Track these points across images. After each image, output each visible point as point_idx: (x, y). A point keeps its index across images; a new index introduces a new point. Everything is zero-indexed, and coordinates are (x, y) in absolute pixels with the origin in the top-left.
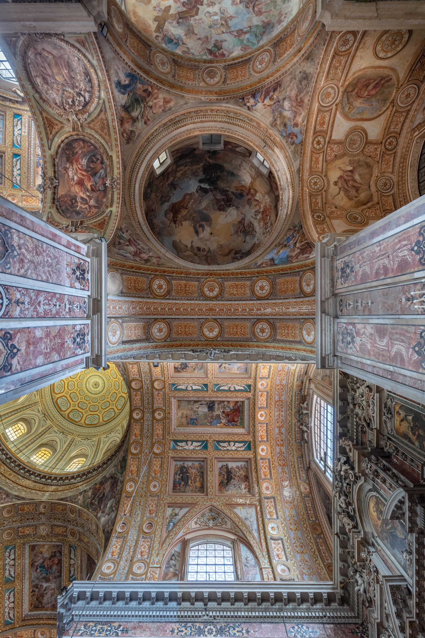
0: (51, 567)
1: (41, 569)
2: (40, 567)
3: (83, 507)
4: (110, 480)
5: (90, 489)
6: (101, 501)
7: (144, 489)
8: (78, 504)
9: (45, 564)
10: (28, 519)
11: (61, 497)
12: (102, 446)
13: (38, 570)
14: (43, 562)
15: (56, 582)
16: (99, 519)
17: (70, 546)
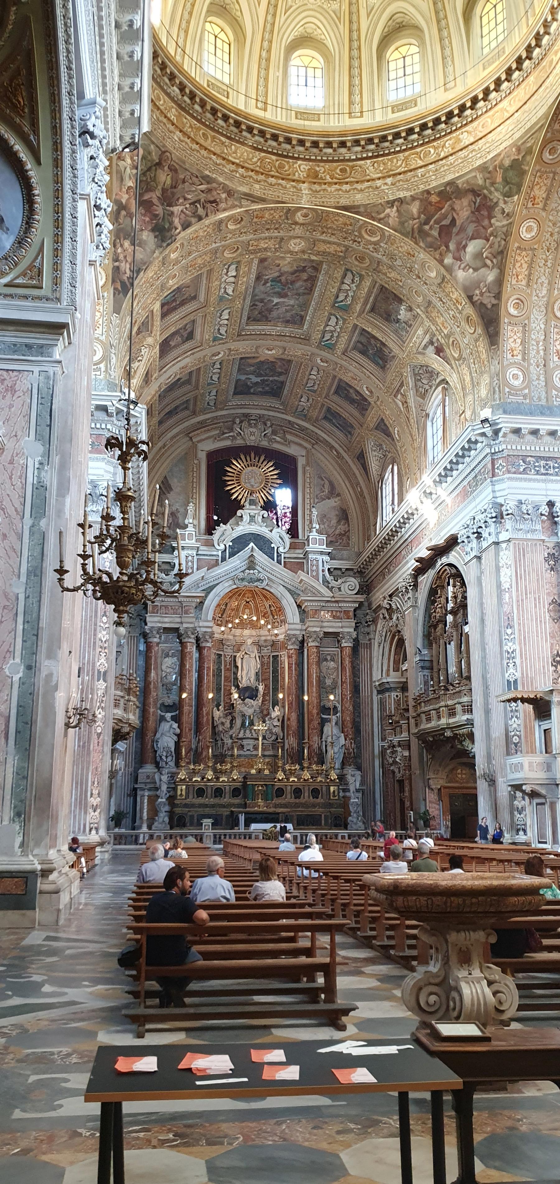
0: (293, 282)
1: (273, 283)
2: (272, 281)
3: (402, 234)
4: (470, 197)
5: (413, 198)
6: (446, 231)
7: (556, 236)
8: (387, 225)
9: (283, 279)
10: (267, 229)
11: (343, 202)
12: (364, 24)
13: (268, 285)
14: (278, 277)
15: (297, 299)
16: (449, 269)
17: (347, 270)
